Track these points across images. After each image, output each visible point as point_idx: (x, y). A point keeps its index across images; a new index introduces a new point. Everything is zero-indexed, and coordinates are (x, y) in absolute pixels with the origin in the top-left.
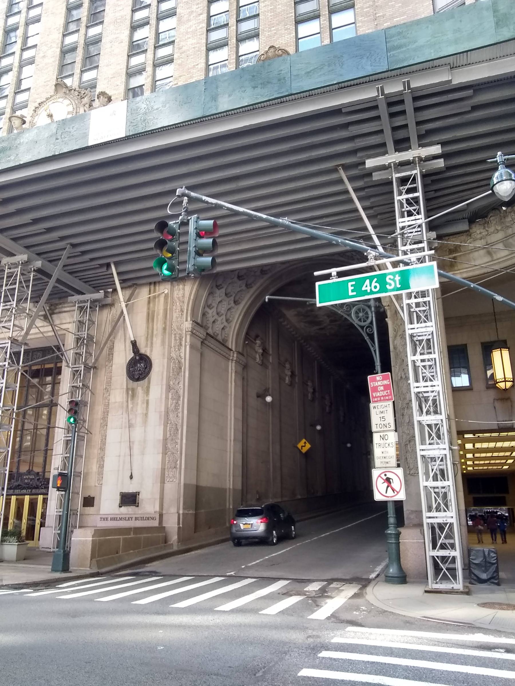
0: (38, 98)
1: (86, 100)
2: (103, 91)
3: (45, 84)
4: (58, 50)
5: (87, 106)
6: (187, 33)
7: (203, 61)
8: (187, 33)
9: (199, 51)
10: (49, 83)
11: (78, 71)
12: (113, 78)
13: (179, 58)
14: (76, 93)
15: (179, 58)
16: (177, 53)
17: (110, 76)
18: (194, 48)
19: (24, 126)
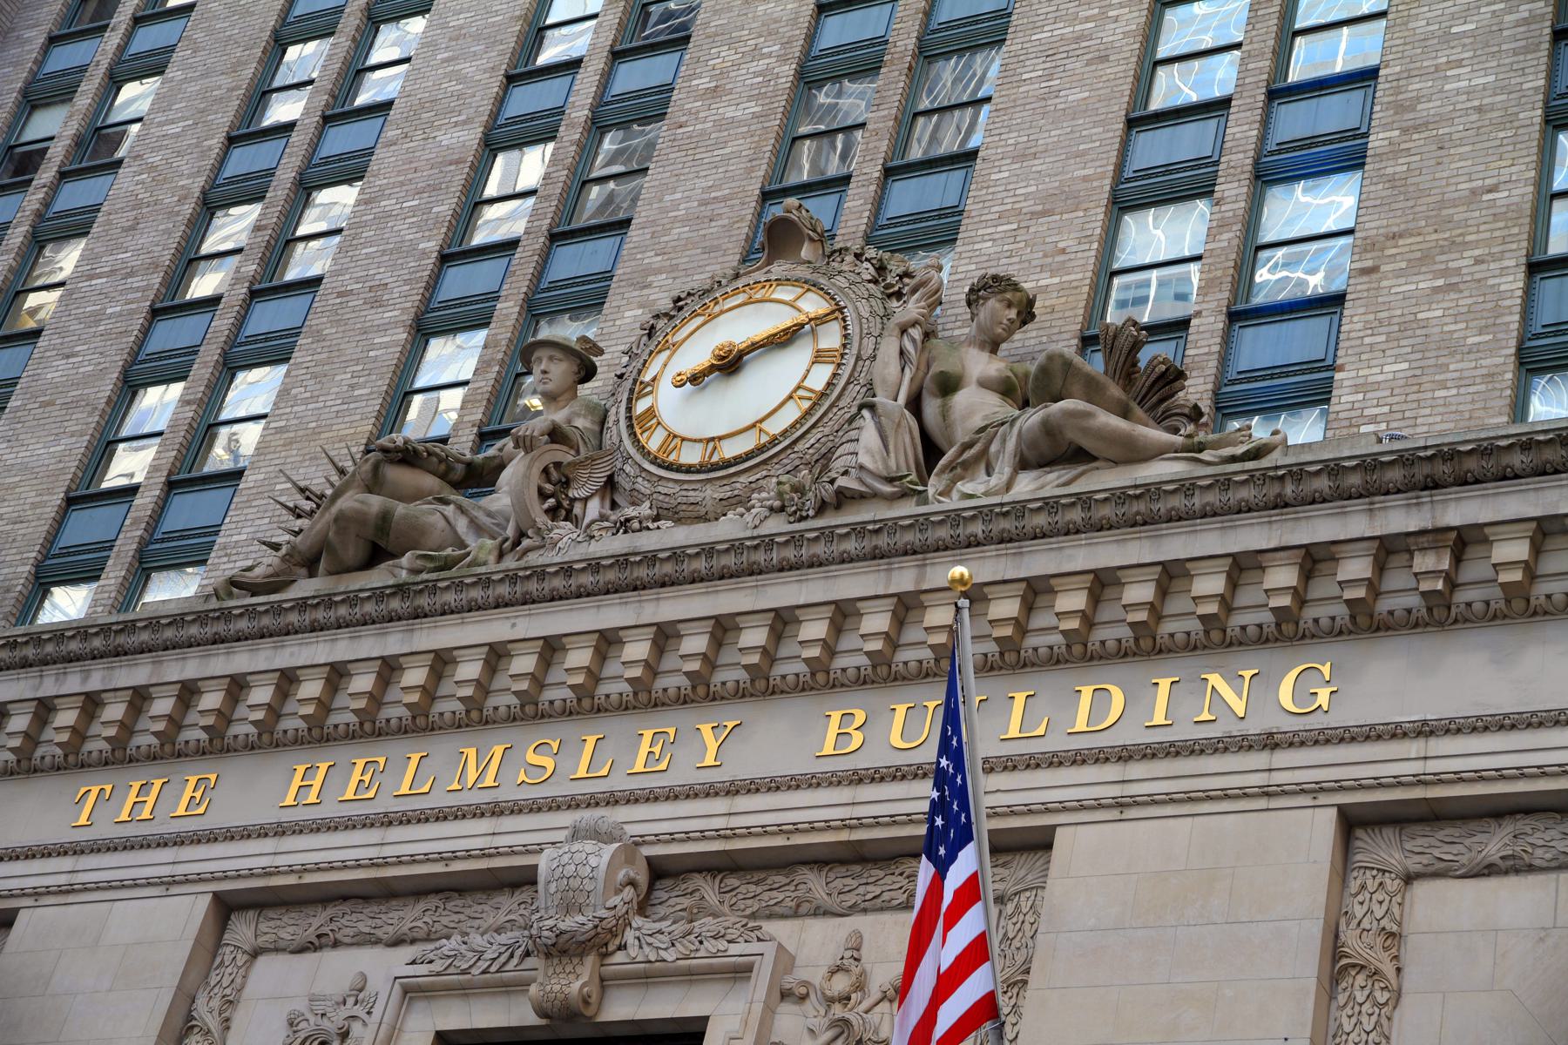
0: (659, 271)
1: (912, 308)
2: (1001, 271)
3: (706, 211)
4: (788, 71)
5: (916, 333)
6: (1447, 38)
7: (1525, 171)
8: (1447, 38)
9: (1501, 126)
10: (720, 208)
11: (875, 171)
12: (1044, 213)
13: (1395, 151)
14: (867, 271)
15: (1395, 151)
16: (1386, 127)
17: (1028, 206)
18: (1479, 109)
19: (585, 390)
